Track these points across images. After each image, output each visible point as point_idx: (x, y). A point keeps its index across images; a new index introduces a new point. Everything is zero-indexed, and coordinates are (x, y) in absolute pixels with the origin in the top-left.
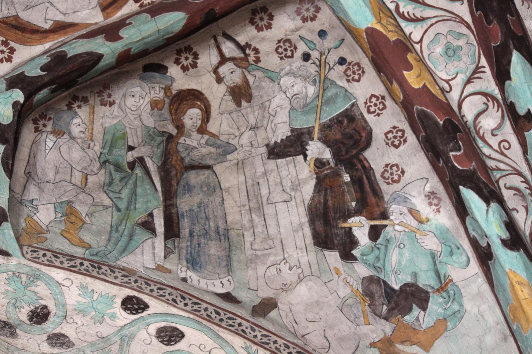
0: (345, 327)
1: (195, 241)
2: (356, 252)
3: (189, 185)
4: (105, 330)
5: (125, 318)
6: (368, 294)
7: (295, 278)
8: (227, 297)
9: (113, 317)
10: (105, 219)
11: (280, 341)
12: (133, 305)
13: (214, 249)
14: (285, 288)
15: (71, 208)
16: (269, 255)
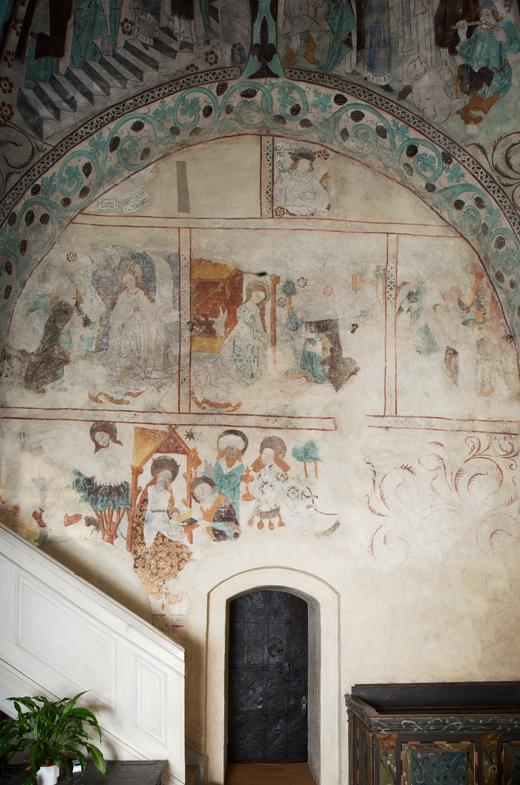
0: (446, 101)
1: (373, 50)
2: (458, 48)
3: (370, 7)
4: (327, 115)
5: (336, 107)
6: (460, 77)
7: (422, 71)
8: (387, 88)
9: (330, 107)
10: (326, 41)
11: (411, 115)
12: (340, 100)
13: (382, 55)
14: (418, 78)
15: (309, 35)
16: (410, 55)
